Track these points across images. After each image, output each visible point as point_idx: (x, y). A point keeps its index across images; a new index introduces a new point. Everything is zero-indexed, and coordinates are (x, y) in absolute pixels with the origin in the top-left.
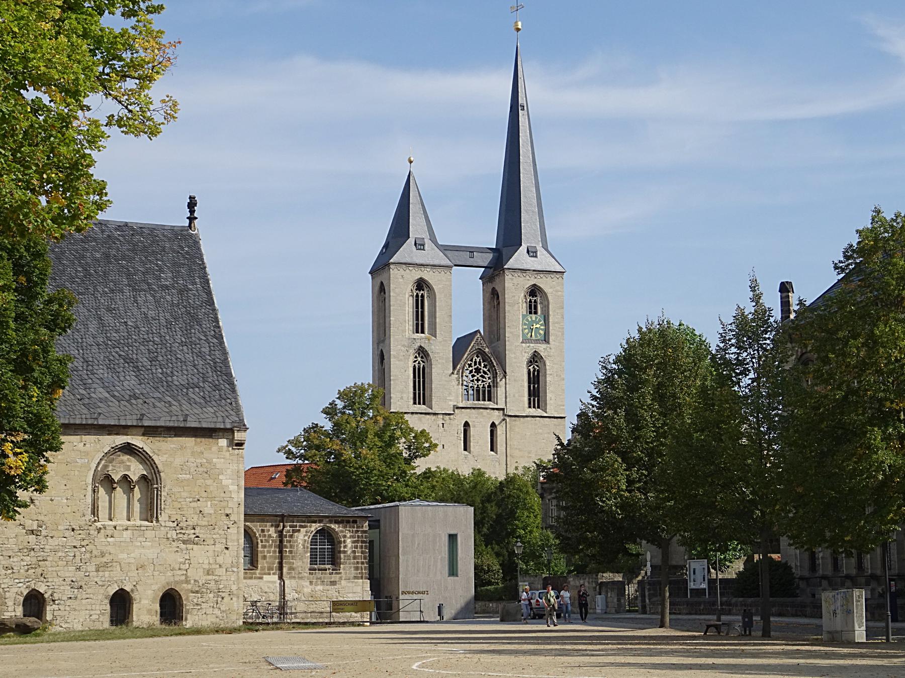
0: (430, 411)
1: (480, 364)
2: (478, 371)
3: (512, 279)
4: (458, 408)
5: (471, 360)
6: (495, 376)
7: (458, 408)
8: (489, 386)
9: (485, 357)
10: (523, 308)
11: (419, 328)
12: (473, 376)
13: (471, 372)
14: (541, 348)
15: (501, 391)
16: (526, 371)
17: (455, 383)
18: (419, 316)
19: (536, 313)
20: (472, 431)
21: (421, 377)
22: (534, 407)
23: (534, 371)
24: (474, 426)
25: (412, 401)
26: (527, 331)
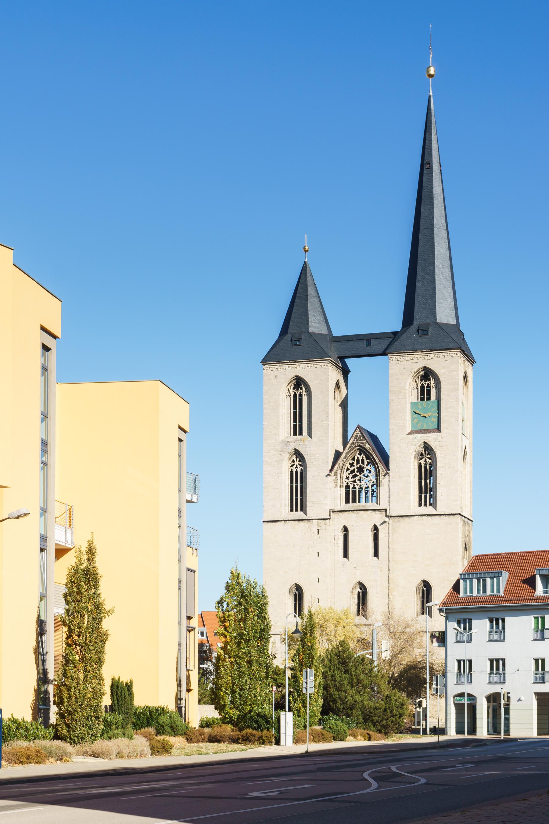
0: (304, 517)
3: (397, 364)
4: (334, 512)
7: (334, 512)
10: (413, 395)
11: (297, 430)
12: (355, 476)
14: (431, 439)
15: (383, 490)
18: (297, 417)
19: (429, 399)
22: (425, 505)
23: (426, 464)
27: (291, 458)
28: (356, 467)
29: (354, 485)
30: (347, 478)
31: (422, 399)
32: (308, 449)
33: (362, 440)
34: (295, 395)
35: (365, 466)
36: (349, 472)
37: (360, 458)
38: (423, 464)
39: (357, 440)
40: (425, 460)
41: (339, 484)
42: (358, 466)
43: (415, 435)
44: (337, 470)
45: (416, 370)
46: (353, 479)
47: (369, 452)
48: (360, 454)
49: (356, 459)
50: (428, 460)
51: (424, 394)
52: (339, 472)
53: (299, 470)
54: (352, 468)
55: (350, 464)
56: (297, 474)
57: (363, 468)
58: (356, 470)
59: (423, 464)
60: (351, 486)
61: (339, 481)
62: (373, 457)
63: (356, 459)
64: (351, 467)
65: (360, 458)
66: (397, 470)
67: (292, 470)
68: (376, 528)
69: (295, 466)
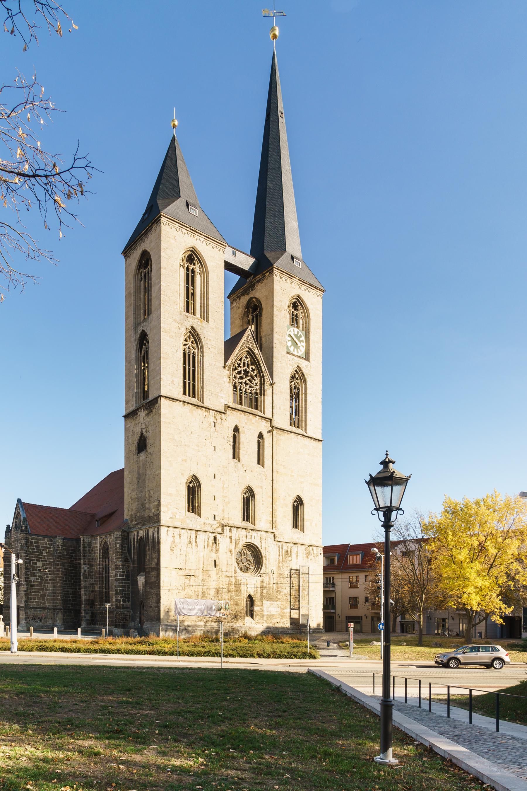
2: (246, 373)
5: (240, 360)
6: (262, 384)
8: (256, 393)
9: (255, 361)
12: (241, 378)
13: (239, 373)
16: (289, 386)
20: (243, 438)
21: (191, 365)
23: (295, 388)
24: (244, 433)
25: (181, 390)
29: (241, 387)
30: (235, 377)
33: (252, 343)
36: (236, 371)
39: (248, 342)
42: (244, 368)
44: (230, 366)
46: (240, 381)
55: (237, 363)
57: (248, 372)
59: (293, 386)
60: (239, 387)
62: (259, 365)
64: (238, 367)
66: (279, 384)
68: (261, 436)
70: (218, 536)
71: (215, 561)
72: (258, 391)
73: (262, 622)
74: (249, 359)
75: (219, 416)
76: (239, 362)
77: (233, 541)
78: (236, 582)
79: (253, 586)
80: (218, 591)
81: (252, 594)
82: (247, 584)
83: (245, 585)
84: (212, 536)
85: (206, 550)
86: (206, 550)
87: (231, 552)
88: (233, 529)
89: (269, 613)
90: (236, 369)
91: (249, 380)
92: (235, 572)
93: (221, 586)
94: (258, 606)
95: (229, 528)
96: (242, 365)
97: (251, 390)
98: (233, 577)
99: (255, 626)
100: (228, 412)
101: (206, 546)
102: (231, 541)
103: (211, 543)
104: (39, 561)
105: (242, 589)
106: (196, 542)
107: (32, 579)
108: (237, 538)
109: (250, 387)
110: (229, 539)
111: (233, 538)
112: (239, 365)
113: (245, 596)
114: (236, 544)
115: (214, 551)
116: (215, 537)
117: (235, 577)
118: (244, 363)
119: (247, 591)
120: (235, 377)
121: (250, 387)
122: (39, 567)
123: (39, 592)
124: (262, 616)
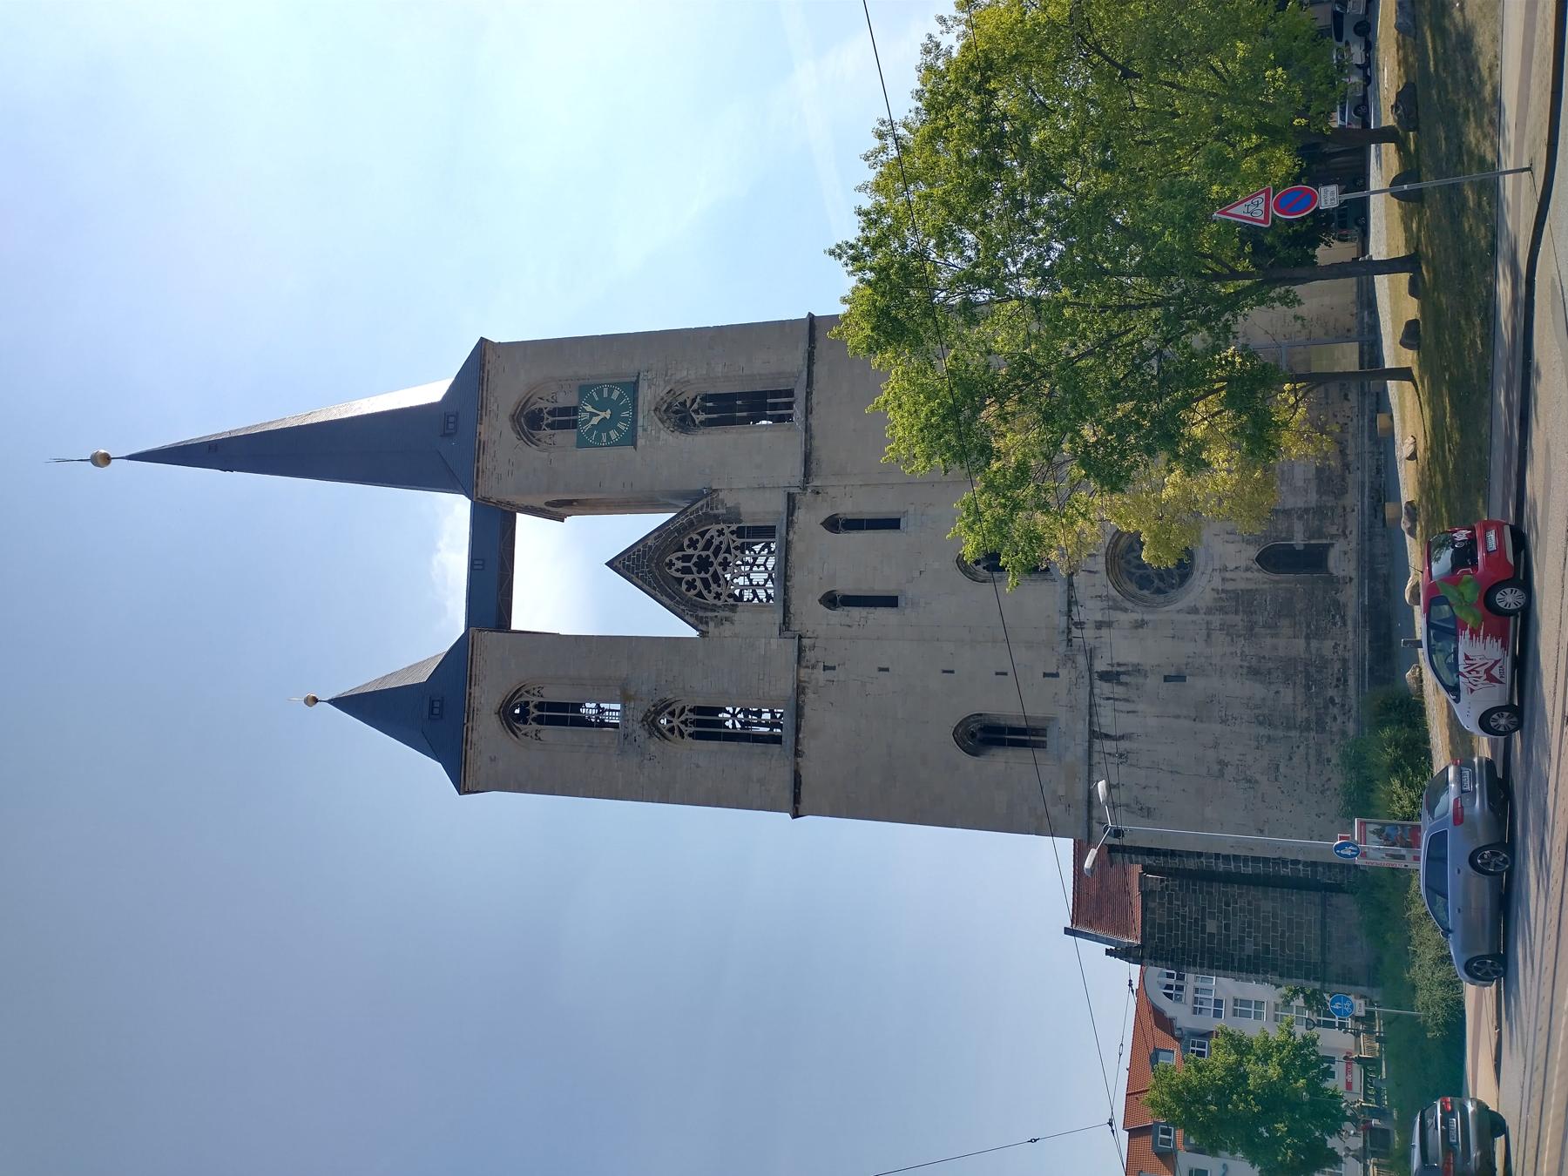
1: (687, 558)
2: (703, 564)
4: (786, 624)
6: (716, 519)
8: (740, 532)
17: (727, 629)
19: (575, 410)
26: (613, 434)
27: (663, 735)
28: (696, 576)
31: (574, 425)
32: (644, 689)
34: (539, 720)
35: (697, 553)
36: (705, 593)
37: (679, 564)
38: (703, 417)
40: (696, 412)
41: (727, 614)
42: (694, 569)
43: (640, 430)
45: (514, 436)
47: (665, 540)
48: (671, 564)
49: (679, 575)
50: (695, 406)
51: (566, 418)
52: (701, 614)
53: (693, 717)
54: (698, 583)
56: (698, 723)
58: (703, 575)
61: (721, 614)
62: (677, 530)
63: (679, 575)
65: (679, 564)
67: (690, 735)
69: (683, 727)
70: (1100, 666)
71: (1167, 679)
72: (734, 527)
73: (1340, 510)
74: (673, 557)
75: (809, 655)
76: (684, 587)
77: (1106, 619)
78: (1221, 610)
79: (1231, 548)
80: (1254, 672)
81: (1253, 552)
82: (1225, 569)
83: (1228, 575)
84: (1103, 688)
85: (1140, 707)
86: (1140, 707)
87: (1140, 624)
88: (1076, 619)
89: (1313, 486)
90: (700, 595)
91: (716, 554)
92: (1194, 610)
93: (1237, 661)
94: (1290, 531)
95: (1076, 632)
96: (689, 577)
97: (736, 548)
98: (1210, 618)
99: (1354, 538)
100: (795, 626)
101: (1130, 707)
102: (1109, 624)
103: (1119, 691)
104: (1204, 927)
105: (1242, 585)
106: (1122, 737)
107: (1250, 948)
108: (1099, 604)
109: (728, 551)
110: (1104, 632)
111: (1099, 617)
112: (691, 585)
113: (1260, 579)
114: (1116, 607)
115: (1141, 680)
116: (1106, 676)
117: (1209, 611)
118: (686, 570)
119: (1247, 569)
120: (718, 596)
121: (728, 551)
122: (1219, 927)
123: (1283, 935)
124: (1320, 511)
